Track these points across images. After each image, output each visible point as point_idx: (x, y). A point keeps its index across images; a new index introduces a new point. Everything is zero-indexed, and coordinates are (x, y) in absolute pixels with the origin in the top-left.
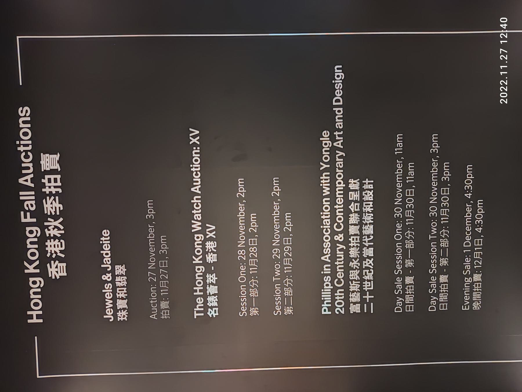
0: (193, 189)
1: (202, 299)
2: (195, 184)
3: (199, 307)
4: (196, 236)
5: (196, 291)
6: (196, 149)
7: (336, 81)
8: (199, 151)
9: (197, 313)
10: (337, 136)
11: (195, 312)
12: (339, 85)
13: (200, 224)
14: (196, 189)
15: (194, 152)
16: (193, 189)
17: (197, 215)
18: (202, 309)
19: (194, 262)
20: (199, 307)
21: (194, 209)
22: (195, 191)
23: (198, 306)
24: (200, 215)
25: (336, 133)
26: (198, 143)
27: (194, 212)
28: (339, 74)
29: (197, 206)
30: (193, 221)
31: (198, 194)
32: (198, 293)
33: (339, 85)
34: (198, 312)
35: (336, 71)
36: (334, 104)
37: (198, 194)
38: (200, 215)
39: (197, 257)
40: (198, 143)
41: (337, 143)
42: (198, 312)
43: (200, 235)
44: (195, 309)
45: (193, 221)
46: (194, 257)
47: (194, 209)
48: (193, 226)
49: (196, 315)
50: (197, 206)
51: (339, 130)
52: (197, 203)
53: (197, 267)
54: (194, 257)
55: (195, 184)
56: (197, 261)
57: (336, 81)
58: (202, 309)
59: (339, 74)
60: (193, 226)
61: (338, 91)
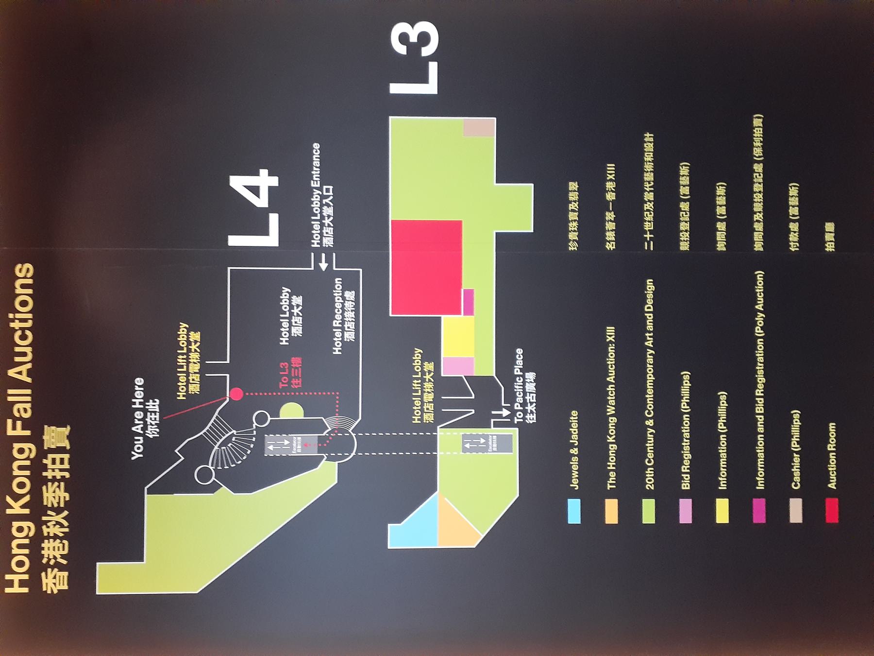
0: (608, 379)
1: (614, 473)
2: (610, 374)
3: (612, 480)
4: (610, 418)
5: (609, 466)
6: (612, 346)
7: (648, 292)
8: (613, 348)
9: (610, 485)
10: (648, 337)
11: (608, 484)
12: (650, 296)
13: (614, 408)
14: (611, 379)
15: (610, 348)
16: (608, 379)
17: (611, 401)
18: (614, 482)
19: (608, 441)
20: (612, 480)
21: (609, 396)
22: (610, 381)
23: (611, 479)
24: (614, 401)
25: (647, 335)
26: (613, 340)
27: (609, 398)
28: (650, 286)
29: (612, 393)
30: (608, 406)
31: (612, 383)
32: (611, 468)
33: (650, 296)
34: (611, 484)
35: (648, 283)
36: (646, 310)
37: (612, 383)
38: (614, 401)
39: (611, 436)
40: (613, 340)
41: (648, 342)
42: (611, 484)
43: (613, 418)
44: (608, 482)
45: (608, 406)
46: (608, 437)
47: (609, 396)
48: (608, 410)
49: (609, 487)
50: (612, 393)
51: (650, 332)
52: (612, 391)
53: (611, 445)
54: (608, 437)
55: (610, 374)
56: (611, 440)
57: (648, 292)
58: (614, 482)
59: (650, 286)
60: (608, 410)
61: (649, 300)
